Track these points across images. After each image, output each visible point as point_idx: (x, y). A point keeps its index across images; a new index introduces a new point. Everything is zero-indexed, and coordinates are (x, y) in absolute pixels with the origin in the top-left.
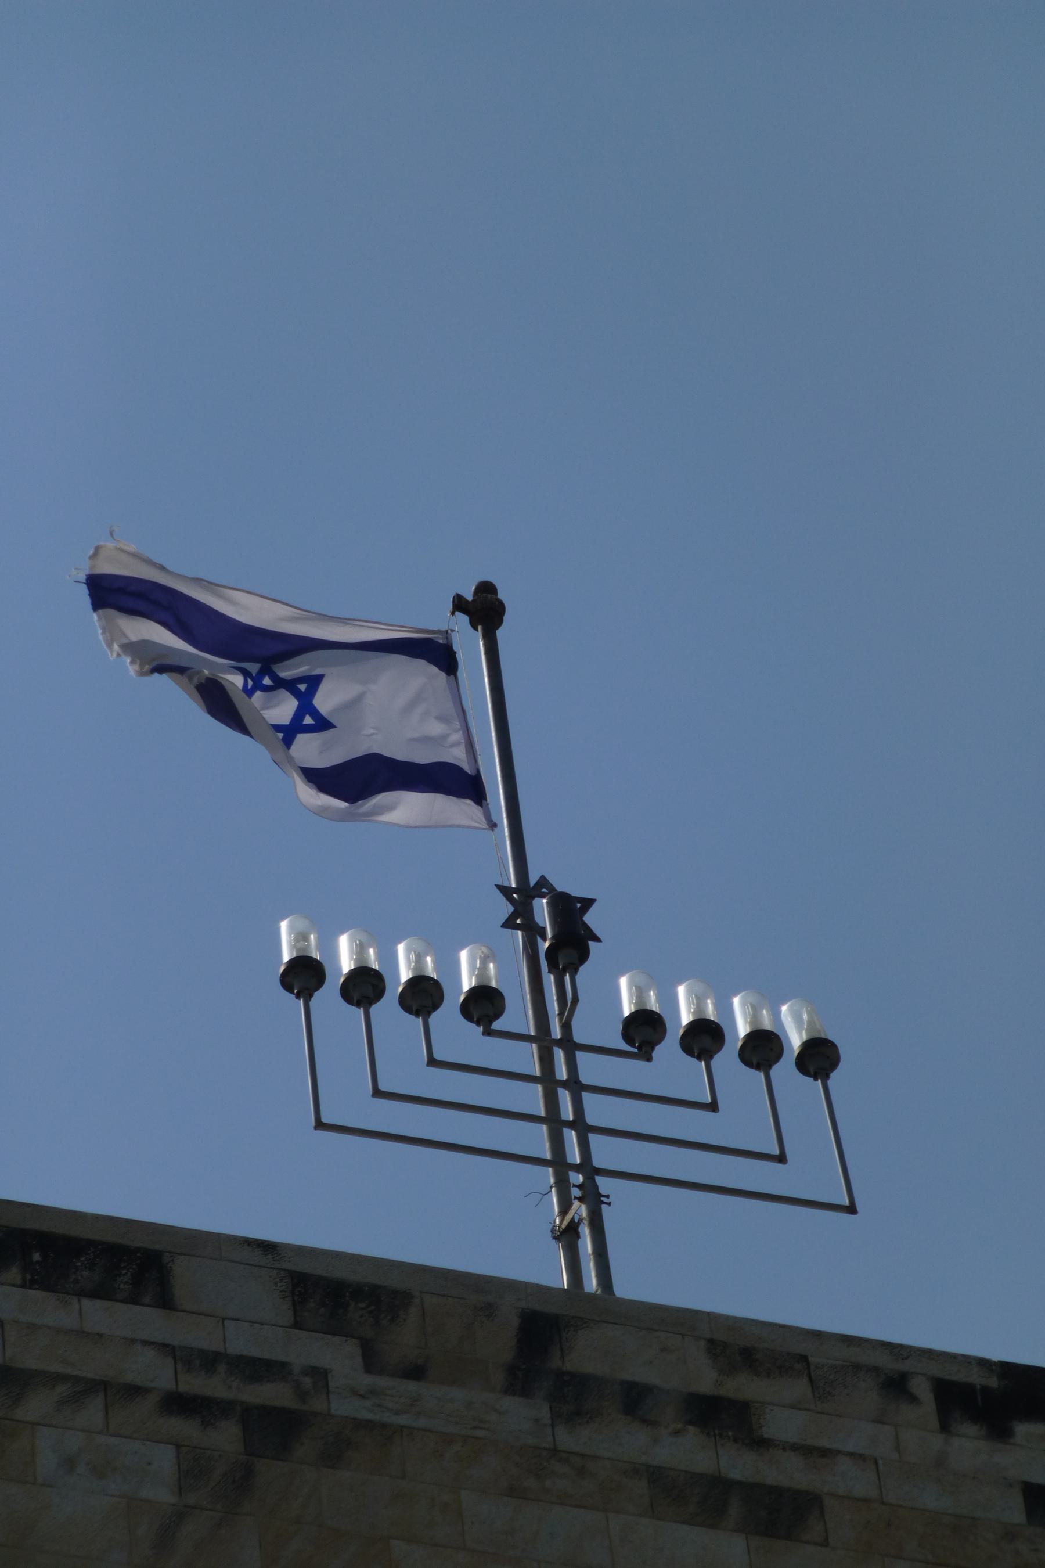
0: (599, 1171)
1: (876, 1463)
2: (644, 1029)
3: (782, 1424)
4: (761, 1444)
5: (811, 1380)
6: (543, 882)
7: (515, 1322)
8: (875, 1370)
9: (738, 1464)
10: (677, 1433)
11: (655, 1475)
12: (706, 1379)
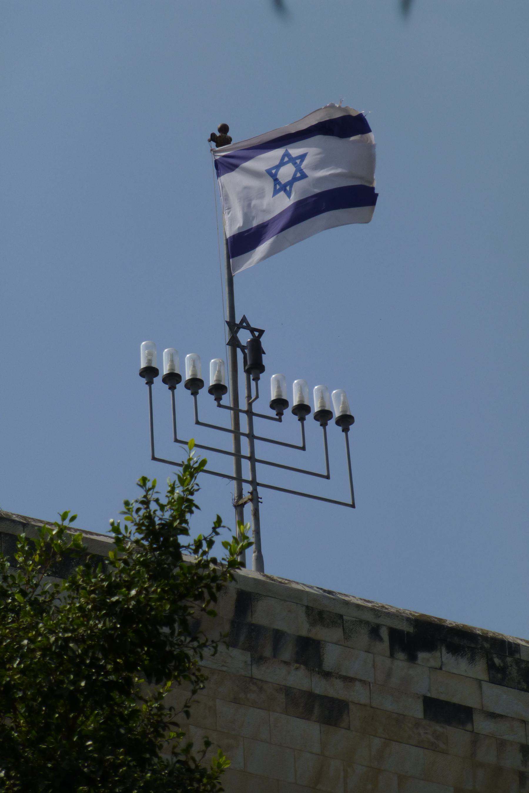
0: (258, 484)
1: (370, 685)
2: (279, 404)
3: (331, 656)
4: (327, 675)
5: (344, 629)
6: (244, 320)
7: (235, 596)
8: (368, 623)
9: (320, 687)
10: (297, 669)
11: (287, 691)
12: (303, 627)
